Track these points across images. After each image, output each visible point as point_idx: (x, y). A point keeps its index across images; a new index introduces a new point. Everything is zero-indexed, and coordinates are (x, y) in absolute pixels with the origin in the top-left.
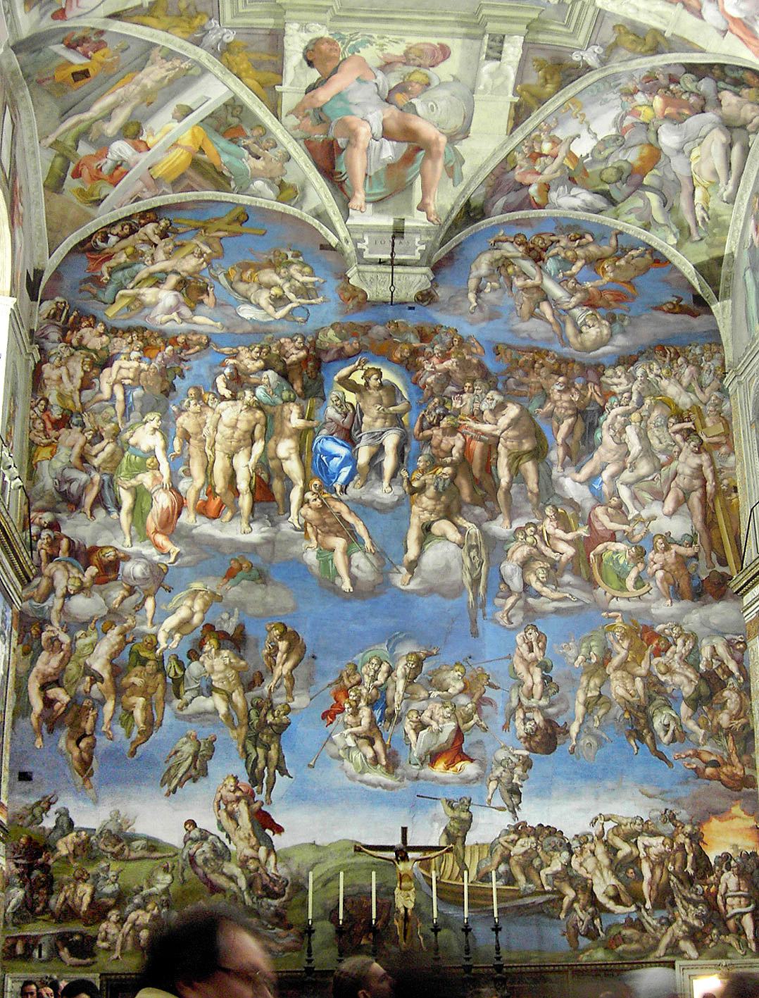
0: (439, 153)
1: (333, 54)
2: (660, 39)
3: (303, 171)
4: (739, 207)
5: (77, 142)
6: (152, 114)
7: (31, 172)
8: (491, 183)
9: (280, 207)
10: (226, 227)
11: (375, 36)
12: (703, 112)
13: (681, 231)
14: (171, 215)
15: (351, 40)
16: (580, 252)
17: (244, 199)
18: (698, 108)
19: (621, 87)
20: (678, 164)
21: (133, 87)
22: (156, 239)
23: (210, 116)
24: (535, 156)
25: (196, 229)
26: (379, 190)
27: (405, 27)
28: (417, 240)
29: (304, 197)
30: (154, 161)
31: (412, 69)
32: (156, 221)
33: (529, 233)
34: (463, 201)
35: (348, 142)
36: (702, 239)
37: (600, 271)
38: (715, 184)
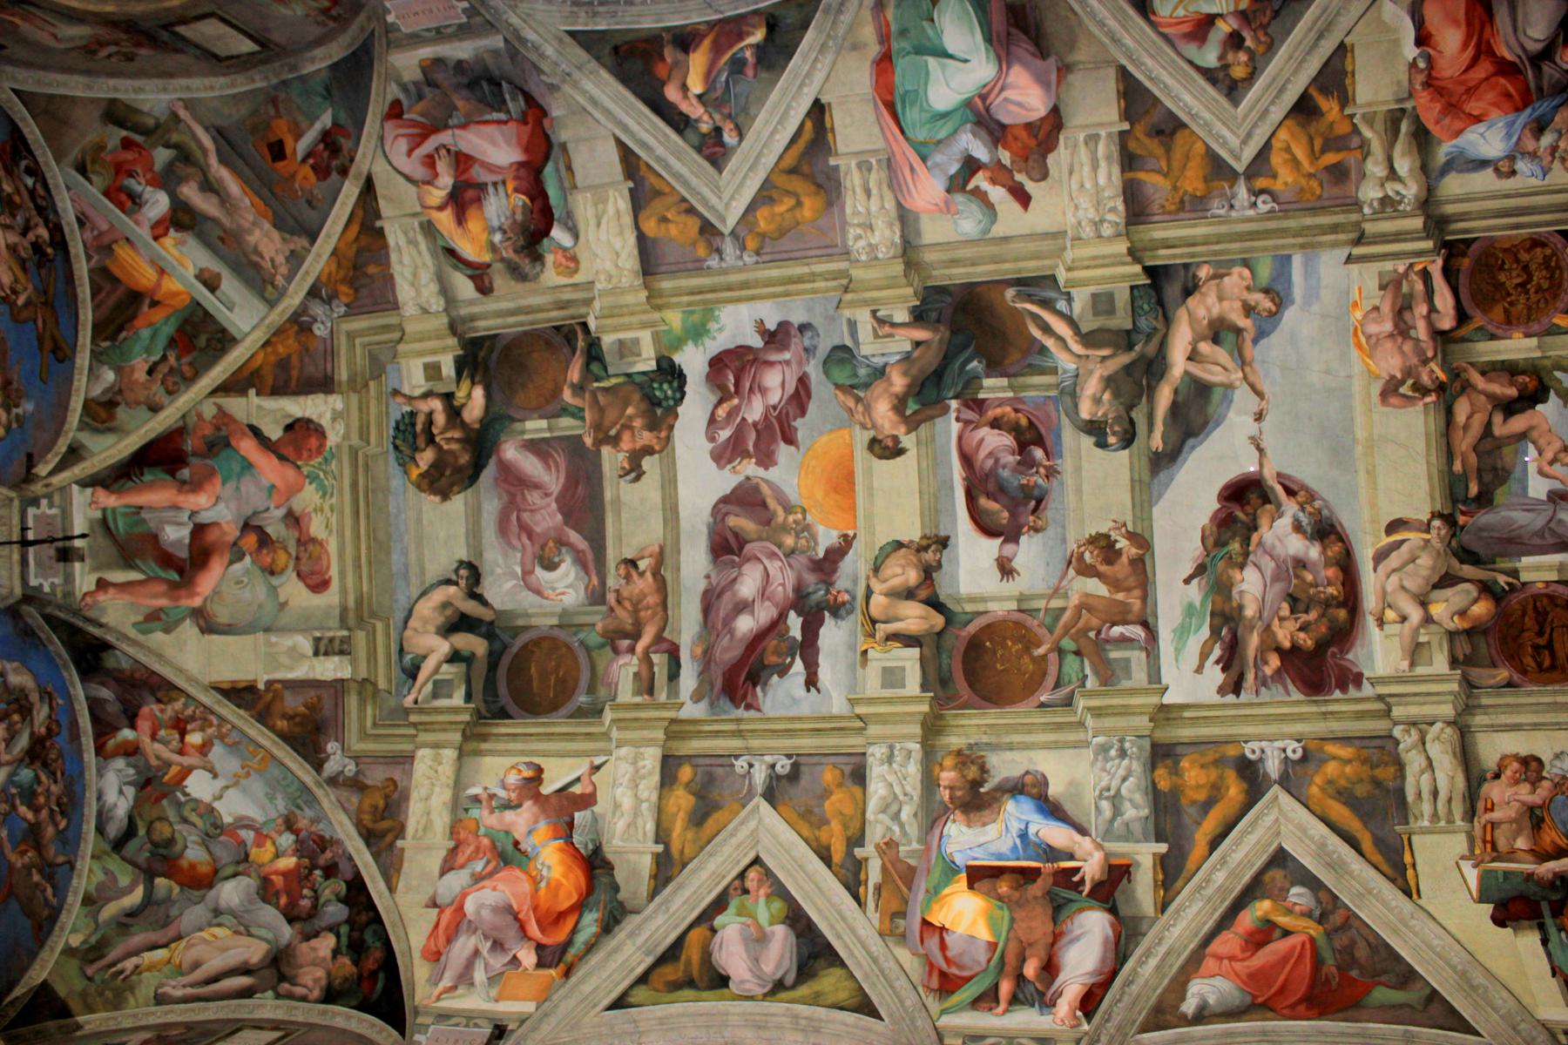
0: (176, 599)
1: (305, 454)
2: (389, 837)
3: (138, 428)
4: (153, 1013)
5: (176, 146)
6: (208, 244)
7: (137, 83)
8: (137, 675)
9: (77, 404)
10: (48, 334)
11: (334, 500)
12: (291, 920)
13: (92, 949)
14: (59, 262)
15: (325, 472)
16: (44, 813)
17: (83, 359)
18: (295, 912)
19: (298, 812)
20: (195, 914)
21: (251, 218)
22: (31, 236)
23: (207, 314)
24: (180, 726)
25: (45, 293)
26: (121, 525)
27: (348, 533)
28: (56, 581)
29: (97, 431)
30: (138, 245)
31: (293, 550)
32: (52, 244)
33: (62, 741)
34: (110, 638)
35: (184, 482)
36: (90, 979)
37: (23, 847)
38: (179, 971)
